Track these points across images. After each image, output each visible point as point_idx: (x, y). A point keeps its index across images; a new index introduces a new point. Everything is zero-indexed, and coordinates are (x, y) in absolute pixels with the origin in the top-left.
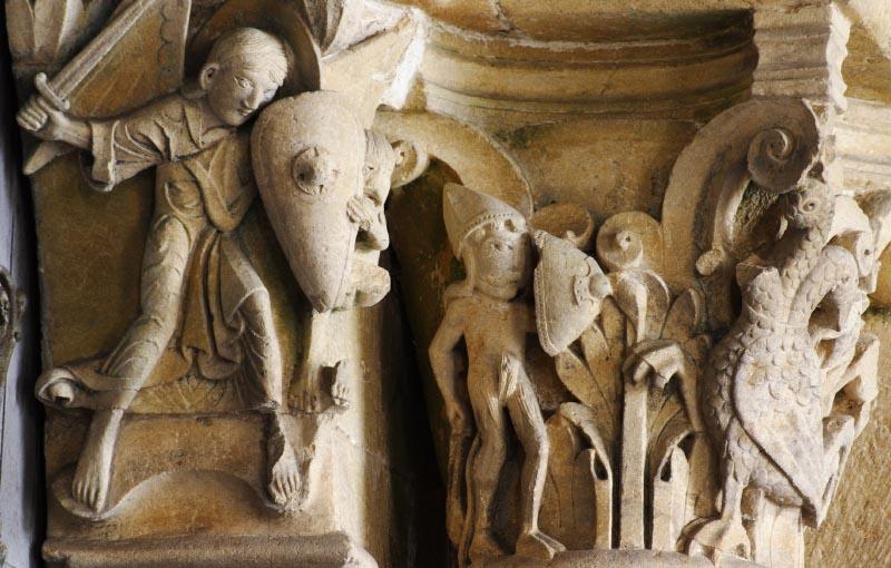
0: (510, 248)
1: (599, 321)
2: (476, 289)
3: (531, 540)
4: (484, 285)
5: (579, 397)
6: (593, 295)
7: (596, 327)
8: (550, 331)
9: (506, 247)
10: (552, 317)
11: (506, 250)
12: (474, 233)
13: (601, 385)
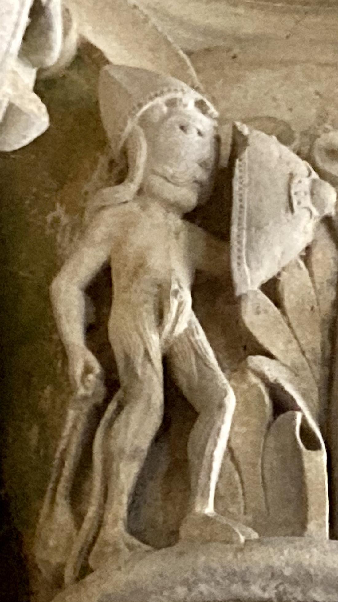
0: (200, 133)
1: (307, 255)
2: (140, 192)
3: (207, 519)
4: (157, 182)
5: (274, 352)
6: (314, 203)
7: (302, 263)
8: (250, 246)
9: (195, 132)
10: (256, 226)
11: (193, 136)
12: (152, 109)
13: (303, 342)
